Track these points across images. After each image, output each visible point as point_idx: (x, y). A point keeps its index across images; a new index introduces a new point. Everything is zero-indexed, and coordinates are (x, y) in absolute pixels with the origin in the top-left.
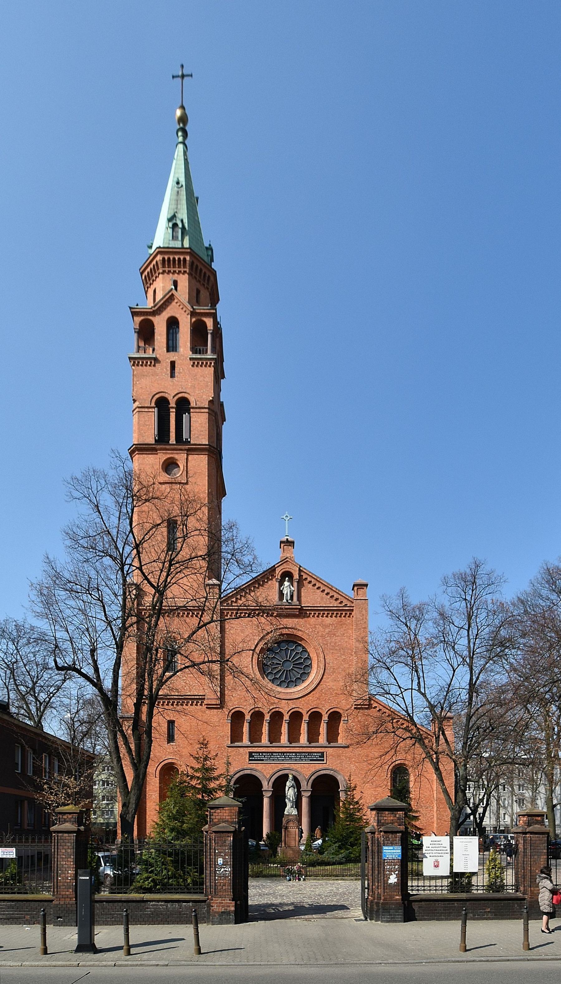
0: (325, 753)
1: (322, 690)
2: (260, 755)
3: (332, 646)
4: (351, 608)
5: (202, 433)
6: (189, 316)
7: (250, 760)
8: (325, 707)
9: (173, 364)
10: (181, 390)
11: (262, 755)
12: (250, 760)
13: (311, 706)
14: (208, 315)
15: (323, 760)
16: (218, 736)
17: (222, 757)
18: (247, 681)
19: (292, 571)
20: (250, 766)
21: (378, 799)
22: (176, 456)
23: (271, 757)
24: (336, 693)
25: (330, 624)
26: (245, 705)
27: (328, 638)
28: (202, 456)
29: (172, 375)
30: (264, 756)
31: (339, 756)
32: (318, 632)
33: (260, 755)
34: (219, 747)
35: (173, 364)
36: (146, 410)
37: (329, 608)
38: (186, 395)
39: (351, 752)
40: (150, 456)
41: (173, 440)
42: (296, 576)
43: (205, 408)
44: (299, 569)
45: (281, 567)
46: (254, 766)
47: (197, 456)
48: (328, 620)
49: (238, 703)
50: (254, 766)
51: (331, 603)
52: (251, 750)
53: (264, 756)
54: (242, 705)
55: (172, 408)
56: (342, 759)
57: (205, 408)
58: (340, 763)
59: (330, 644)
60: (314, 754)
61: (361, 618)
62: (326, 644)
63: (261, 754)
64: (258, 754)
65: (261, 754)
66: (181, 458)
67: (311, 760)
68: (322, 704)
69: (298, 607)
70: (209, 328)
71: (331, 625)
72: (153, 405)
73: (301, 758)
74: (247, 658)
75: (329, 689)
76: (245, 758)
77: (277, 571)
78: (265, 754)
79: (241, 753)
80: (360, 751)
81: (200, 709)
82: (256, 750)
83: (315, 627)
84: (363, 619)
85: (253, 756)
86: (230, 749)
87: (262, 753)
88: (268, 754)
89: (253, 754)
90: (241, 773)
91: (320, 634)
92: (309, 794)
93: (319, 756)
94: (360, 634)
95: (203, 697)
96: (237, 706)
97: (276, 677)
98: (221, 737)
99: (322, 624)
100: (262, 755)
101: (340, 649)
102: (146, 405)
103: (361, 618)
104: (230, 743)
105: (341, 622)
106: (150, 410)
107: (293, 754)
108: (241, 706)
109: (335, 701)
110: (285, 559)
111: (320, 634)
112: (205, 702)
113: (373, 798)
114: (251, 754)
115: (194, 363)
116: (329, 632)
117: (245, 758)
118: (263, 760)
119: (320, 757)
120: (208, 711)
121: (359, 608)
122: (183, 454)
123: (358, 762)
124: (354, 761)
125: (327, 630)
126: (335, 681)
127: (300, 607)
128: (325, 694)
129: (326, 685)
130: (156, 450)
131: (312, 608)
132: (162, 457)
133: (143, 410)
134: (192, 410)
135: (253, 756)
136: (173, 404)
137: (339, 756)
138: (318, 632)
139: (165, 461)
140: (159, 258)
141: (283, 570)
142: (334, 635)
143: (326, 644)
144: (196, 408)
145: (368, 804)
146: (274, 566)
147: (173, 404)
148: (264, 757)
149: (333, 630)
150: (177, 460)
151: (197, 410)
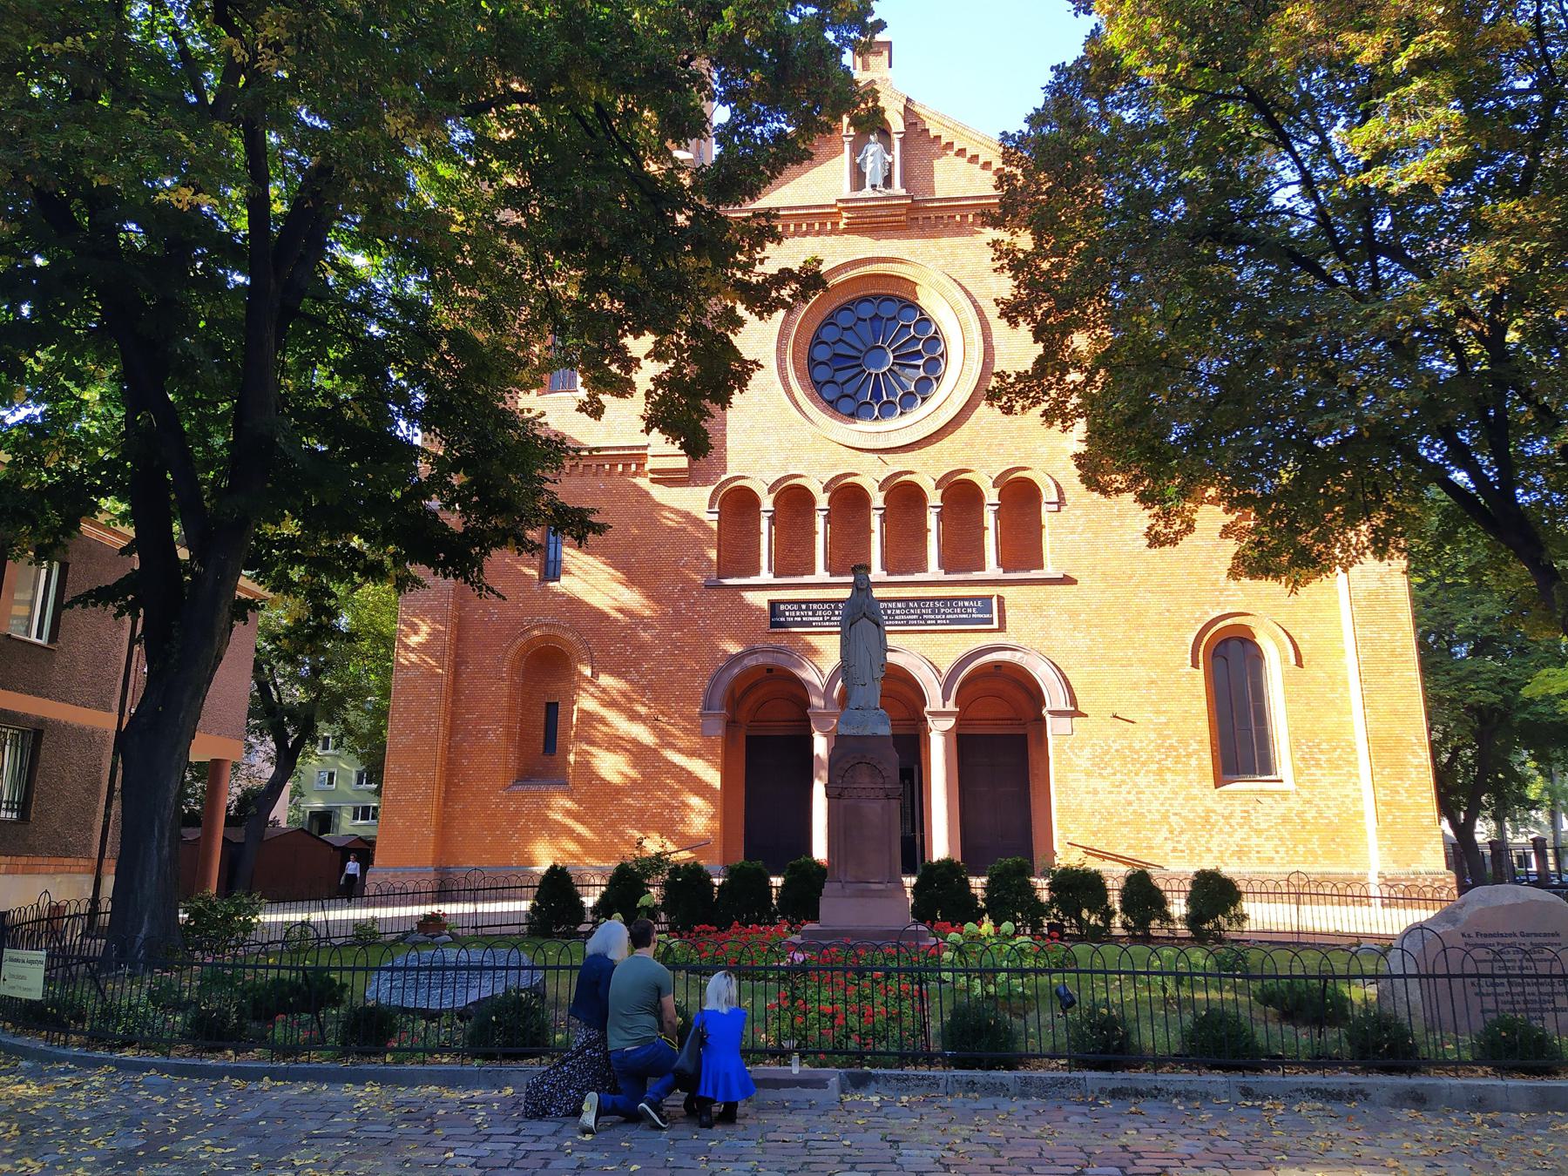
0: (995, 601)
2: (800, 609)
15: (990, 621)
17: (691, 619)
20: (773, 641)
21: (1169, 737)
23: (834, 615)
30: (815, 612)
34: (683, 590)
60: (961, 604)
63: (804, 607)
64: (795, 607)
67: (953, 622)
73: (922, 615)
78: (815, 606)
80: (1103, 592)
88: (826, 606)
92: (950, 723)
93: (977, 608)
97: (846, 392)
107: (899, 605)
109: (1017, 449)
113: (1153, 736)
118: (809, 624)
119: (979, 611)
145: (1137, 753)
148: (814, 616)
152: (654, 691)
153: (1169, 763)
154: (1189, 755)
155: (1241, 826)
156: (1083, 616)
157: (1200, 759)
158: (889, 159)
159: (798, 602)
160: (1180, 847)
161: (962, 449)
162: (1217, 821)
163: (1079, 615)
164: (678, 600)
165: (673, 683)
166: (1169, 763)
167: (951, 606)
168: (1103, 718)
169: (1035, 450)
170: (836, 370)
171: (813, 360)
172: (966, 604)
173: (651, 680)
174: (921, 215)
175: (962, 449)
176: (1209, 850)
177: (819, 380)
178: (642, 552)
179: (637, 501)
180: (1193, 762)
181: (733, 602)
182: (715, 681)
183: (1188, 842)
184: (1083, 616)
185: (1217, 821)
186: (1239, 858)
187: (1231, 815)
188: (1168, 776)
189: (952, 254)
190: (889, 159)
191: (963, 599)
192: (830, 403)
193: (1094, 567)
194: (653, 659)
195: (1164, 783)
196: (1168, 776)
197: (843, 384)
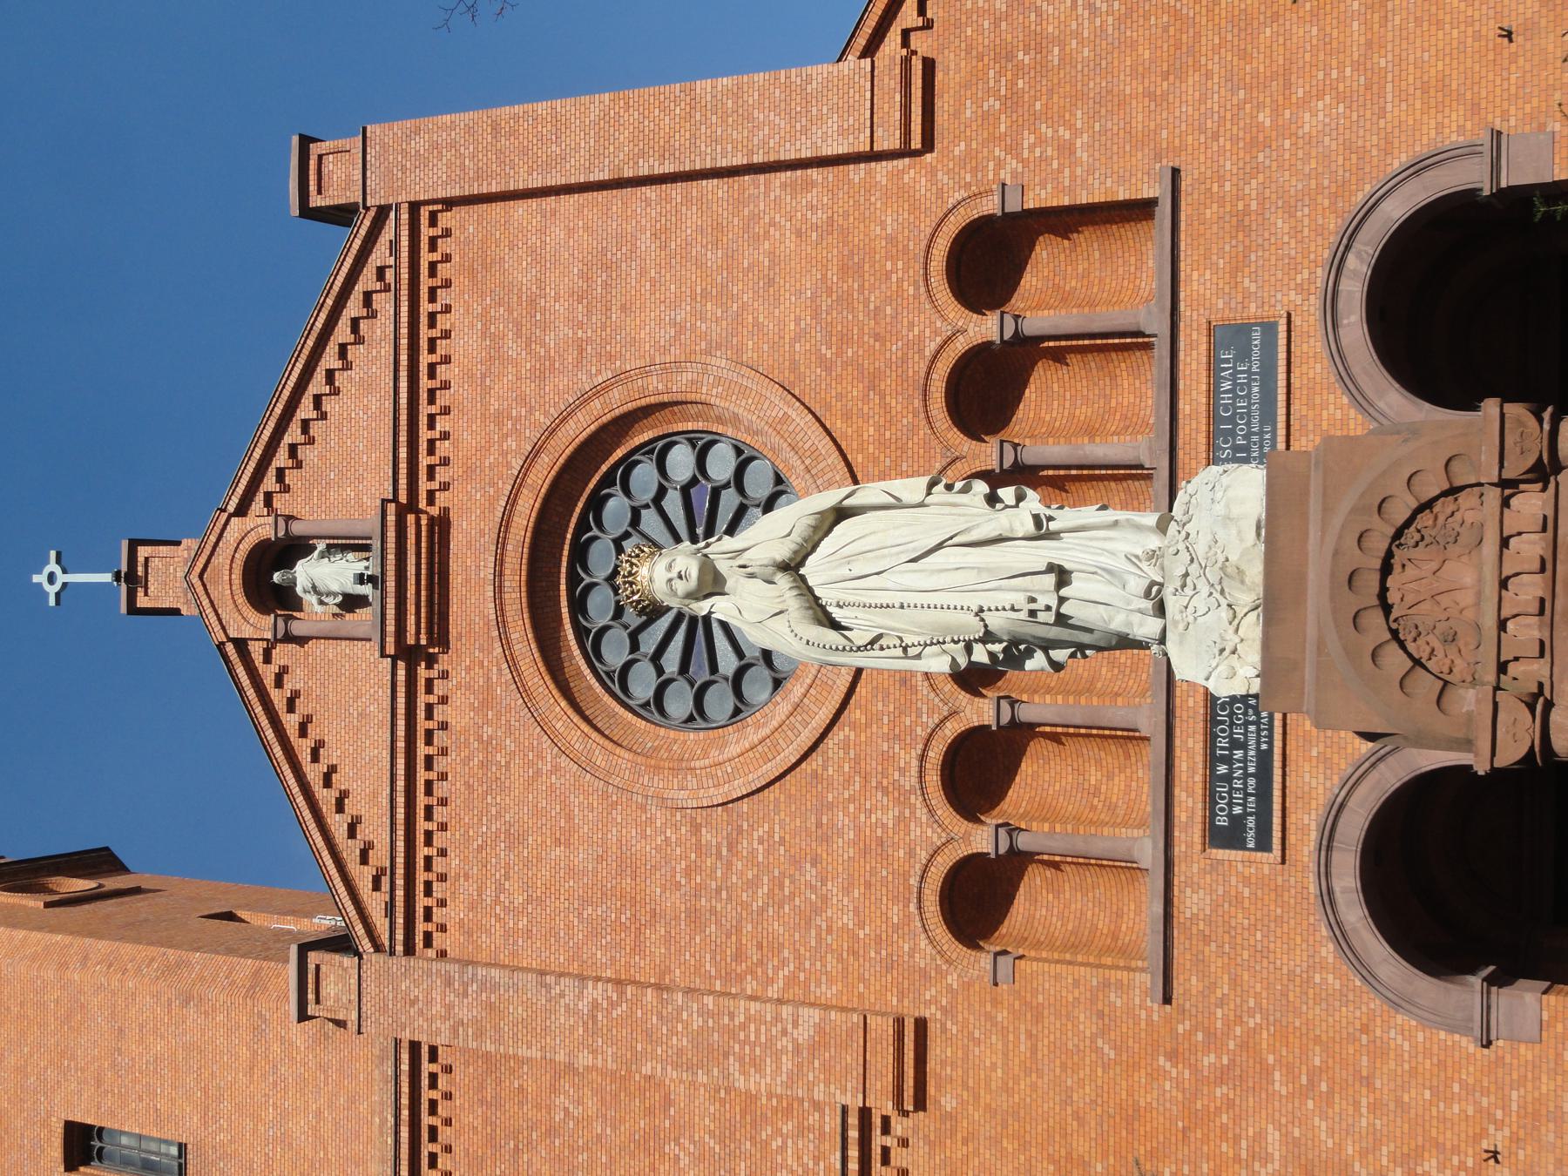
1: (822, 360)
2: (1228, 778)
3: (589, 313)
4: (405, 216)
7: (1264, 845)
8: (920, 338)
11: (1228, 760)
12: (1264, 845)
13: (913, 429)
15: (1269, 328)
16: (1098, 1051)
17: (1244, 1046)
18: (771, 833)
19: (246, 546)
20: (1305, 845)
24: (844, 270)
25: (484, 334)
26: (911, 854)
27: (550, 339)
30: (1235, 744)
31: (1241, 223)
32: (522, 400)
33: (1228, 778)
34: (1173, 1056)
37: (404, 342)
39: (1215, 136)
46: (1306, 824)
48: (465, 345)
49: (895, 900)
50: (1306, 824)
52: (1189, 833)
53: (1235, 744)
54: (906, 876)
56: (1262, 201)
58: (1290, 211)
59: (581, 325)
60: (1226, 399)
61: (448, 155)
62: (581, 351)
65: (1222, 769)
67: (1268, 416)
68: (904, 360)
69: (391, 518)
71: (485, 327)
74: (651, 821)
75: (816, 315)
76: (1246, 881)
77: (247, 632)
79: (1216, 906)
80: (1208, 75)
81: (930, 1144)
82: (1189, 804)
83: (499, 418)
84: (453, 145)
85: (1237, 823)
86: (1186, 982)
87: (1212, 759)
89: (1222, 821)
90: (1355, 913)
91: (529, 388)
94: (525, 152)
95: (853, 1120)
96: (913, 908)
98: (1103, 1032)
99: (484, 376)
100: (1228, 760)
101: (607, 267)
103: (448, 155)
104: (1145, 978)
105: (472, 273)
108: (914, 881)
109: (888, 275)
111: (529, 388)
112: (882, 1105)
114: (1225, 836)
116: (518, 334)
117: (1246, 881)
118: (1265, 759)
119: (1244, 355)
120: (943, 1098)
121: (404, 169)
123: (1287, 85)
124: (1276, 112)
125: (512, 347)
126: (770, 282)
127: (391, 508)
128: (845, 339)
129: (794, 340)
131: (403, 438)
135: (1237, 823)
137: (1241, 223)
138: (522, 400)
141: (241, 599)
142: (532, 302)
143: (581, 351)
148: (1244, 746)
149: (510, 311)
152: (1418, 1154)
156: (1264, 118)
158: (321, 546)
159: (1212, 780)
161: (882, 396)
163: (1260, 127)
164: (1195, 1069)
165: (1399, 1102)
167: (1231, 420)
168: (1513, 59)
169: (891, 240)
170: (714, 668)
171: (691, 719)
172: (1226, 385)
173: (1393, 1159)
174: (424, 485)
175: (882, 396)
177: (730, 709)
178: (1081, 1146)
179: (965, 1142)
181: (1207, 940)
182: (1398, 1003)
184: (1264, 118)
189: (500, 424)
190: (321, 546)
191: (1213, 392)
192: (777, 683)
193: (1151, 96)
194: (1340, 1146)
197: (739, 653)
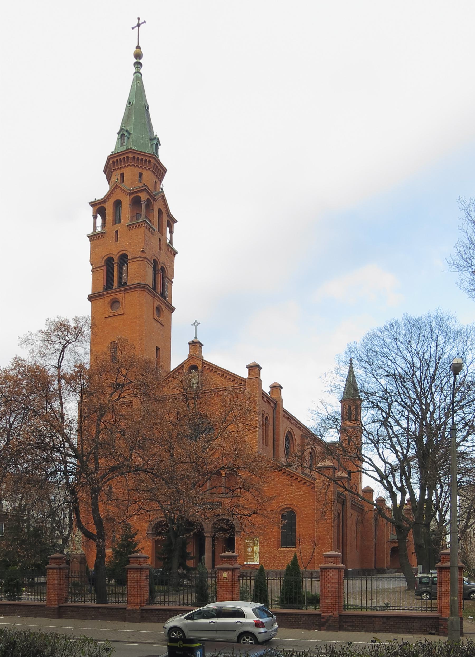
5: (135, 276)
6: (128, 196)
9: (117, 232)
10: (122, 249)
14: (141, 191)
19: (197, 365)
22: (117, 297)
28: (135, 292)
29: (117, 240)
35: (117, 232)
36: (99, 269)
38: (125, 252)
40: (100, 300)
41: (115, 286)
42: (200, 368)
43: (138, 257)
44: (202, 362)
45: (188, 363)
47: (131, 293)
51: (228, 384)
55: (116, 263)
57: (138, 257)
66: (120, 296)
70: (142, 200)
72: (103, 264)
102: (98, 266)
106: (101, 268)
110: (191, 356)
115: (130, 228)
122: (121, 294)
130: (104, 295)
132: (108, 299)
133: (97, 269)
134: (128, 261)
136: (116, 260)
139: (110, 302)
140: (111, 162)
141: (190, 365)
144: (131, 259)
146: (183, 363)
147: (116, 260)
150: (118, 299)
151: (133, 260)
153: (266, 544)
154: (271, 542)
155: (283, 559)
157: (274, 542)
160: (266, 564)
162: (276, 558)
166: (266, 544)
176: (274, 565)
180: (272, 543)
183: (269, 563)
185: (276, 558)
186: (282, 567)
187: (281, 556)
188: (265, 547)
195: (264, 548)
196: (265, 547)
